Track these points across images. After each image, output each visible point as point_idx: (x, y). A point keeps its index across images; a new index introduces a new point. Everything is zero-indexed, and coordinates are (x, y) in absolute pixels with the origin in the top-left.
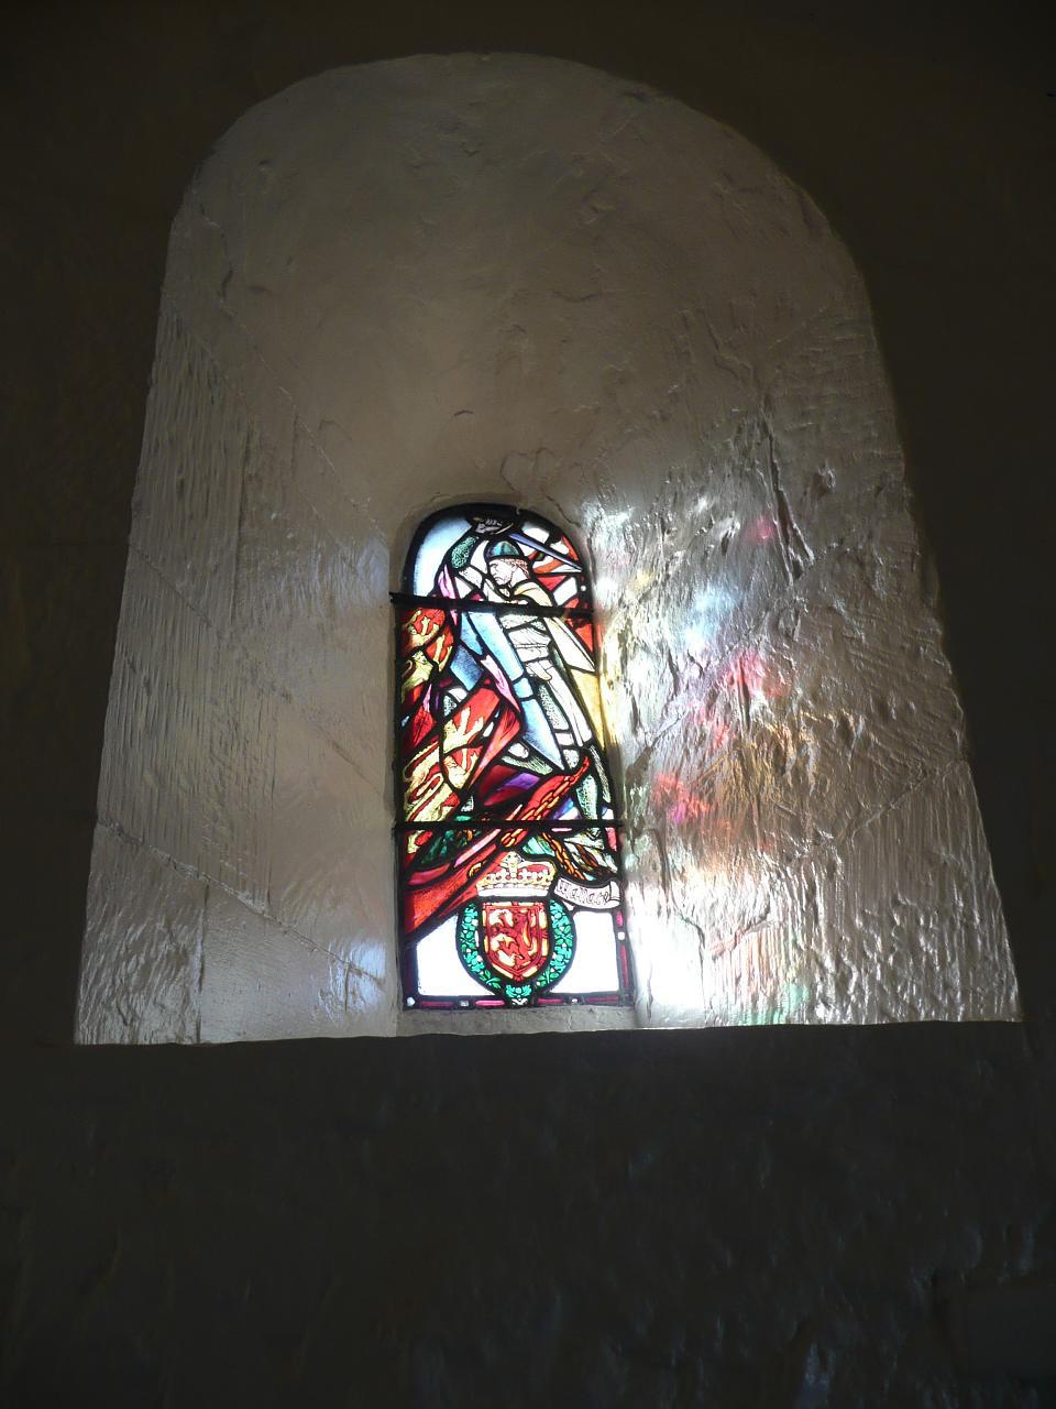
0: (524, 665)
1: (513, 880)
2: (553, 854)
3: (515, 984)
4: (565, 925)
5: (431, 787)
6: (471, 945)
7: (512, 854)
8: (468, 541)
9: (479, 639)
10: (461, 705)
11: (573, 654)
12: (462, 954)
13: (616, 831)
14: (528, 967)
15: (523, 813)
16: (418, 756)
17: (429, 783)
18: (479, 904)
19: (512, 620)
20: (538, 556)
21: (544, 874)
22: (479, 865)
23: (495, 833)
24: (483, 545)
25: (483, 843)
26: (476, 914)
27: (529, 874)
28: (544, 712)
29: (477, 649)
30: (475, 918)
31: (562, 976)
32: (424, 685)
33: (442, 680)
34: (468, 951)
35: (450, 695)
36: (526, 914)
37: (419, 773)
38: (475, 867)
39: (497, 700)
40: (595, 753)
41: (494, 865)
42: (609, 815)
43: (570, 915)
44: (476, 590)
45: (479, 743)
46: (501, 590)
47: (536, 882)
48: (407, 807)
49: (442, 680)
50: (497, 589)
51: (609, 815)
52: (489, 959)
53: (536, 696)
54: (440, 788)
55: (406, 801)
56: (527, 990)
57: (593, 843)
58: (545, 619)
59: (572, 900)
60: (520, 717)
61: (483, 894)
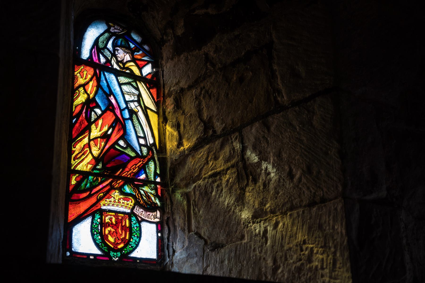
0: (126, 102)
1: (117, 203)
4: (137, 227)
5: (84, 154)
6: (96, 230)
8: (106, 35)
9: (108, 86)
10: (99, 117)
11: (148, 102)
12: (93, 235)
14: (120, 244)
16: (79, 139)
17: (83, 152)
18: (102, 212)
19: (123, 80)
21: (129, 202)
23: (110, 181)
24: (114, 37)
25: (104, 184)
26: (99, 217)
27: (124, 201)
28: (134, 127)
30: (99, 218)
32: (83, 104)
34: (95, 233)
35: (95, 113)
36: (121, 220)
37: (79, 146)
38: (101, 195)
39: (114, 117)
41: (108, 195)
42: (158, 180)
45: (105, 137)
48: (73, 162)
51: (158, 180)
52: (104, 238)
53: (131, 119)
54: (87, 155)
56: (119, 254)
57: (151, 191)
58: (138, 82)
59: (141, 216)
60: (124, 128)
61: (104, 208)
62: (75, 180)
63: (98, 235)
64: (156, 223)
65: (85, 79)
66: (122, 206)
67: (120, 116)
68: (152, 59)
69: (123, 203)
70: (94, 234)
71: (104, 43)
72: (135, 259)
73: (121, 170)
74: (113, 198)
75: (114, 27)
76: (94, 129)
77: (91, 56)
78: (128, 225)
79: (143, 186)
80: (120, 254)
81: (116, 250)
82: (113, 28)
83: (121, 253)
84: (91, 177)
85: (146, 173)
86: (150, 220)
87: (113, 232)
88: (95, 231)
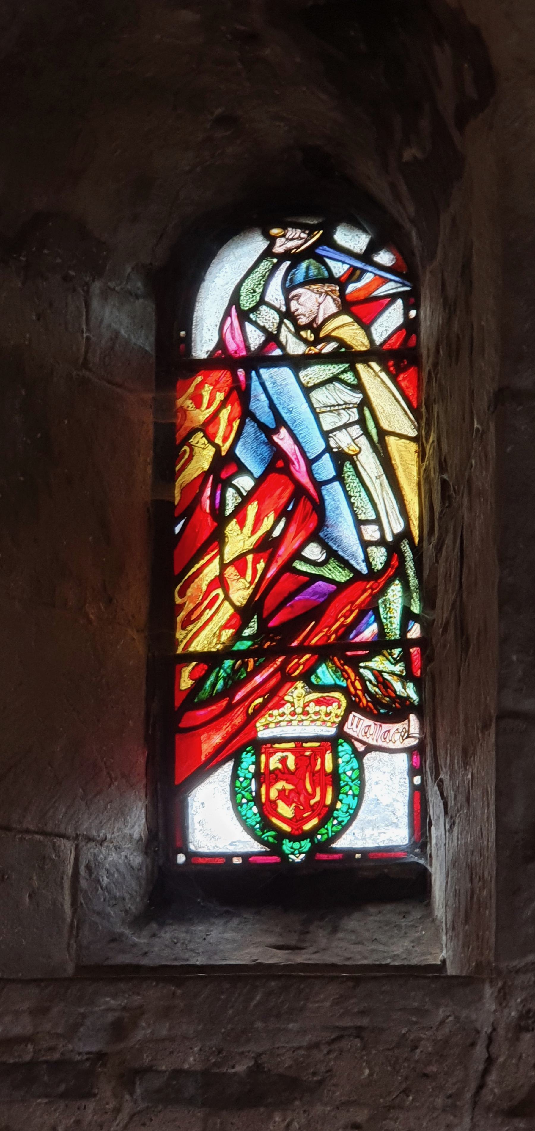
0: (326, 435)
1: (298, 717)
2: (344, 684)
3: (294, 838)
5: (210, 606)
6: (247, 794)
7: (300, 684)
10: (246, 500)
12: (236, 805)
13: (422, 653)
15: (313, 633)
16: (193, 570)
17: (206, 603)
19: (314, 373)
20: (354, 275)
21: (333, 709)
22: (260, 700)
24: (287, 264)
25: (265, 674)
26: (253, 758)
27: (317, 708)
28: (348, 497)
29: (267, 418)
31: (345, 828)
32: (205, 475)
33: (226, 465)
36: (309, 757)
40: (406, 548)
41: (276, 699)
43: (359, 756)
44: (272, 338)
45: (267, 547)
46: (303, 333)
47: (323, 717)
48: (180, 634)
49: (226, 465)
50: (297, 334)
51: (415, 632)
52: (267, 810)
55: (179, 625)
56: (306, 845)
58: (360, 367)
59: (365, 739)
60: (319, 508)
61: (263, 734)
62: (191, 677)
63: (252, 803)
64: (409, 751)
65: (207, 408)
66: (313, 721)
67: (305, 480)
68: (404, 285)
69: (316, 713)
70: (241, 805)
71: (255, 292)
72: (349, 853)
73: (314, 623)
74: (288, 705)
75: (284, 236)
76: (235, 534)
77: (222, 343)
78: (329, 767)
79: (369, 658)
80: (309, 845)
81: (297, 837)
82: (283, 239)
83: (312, 841)
84: (228, 663)
85: (378, 619)
86: (391, 746)
87: (291, 791)
88: (243, 797)
